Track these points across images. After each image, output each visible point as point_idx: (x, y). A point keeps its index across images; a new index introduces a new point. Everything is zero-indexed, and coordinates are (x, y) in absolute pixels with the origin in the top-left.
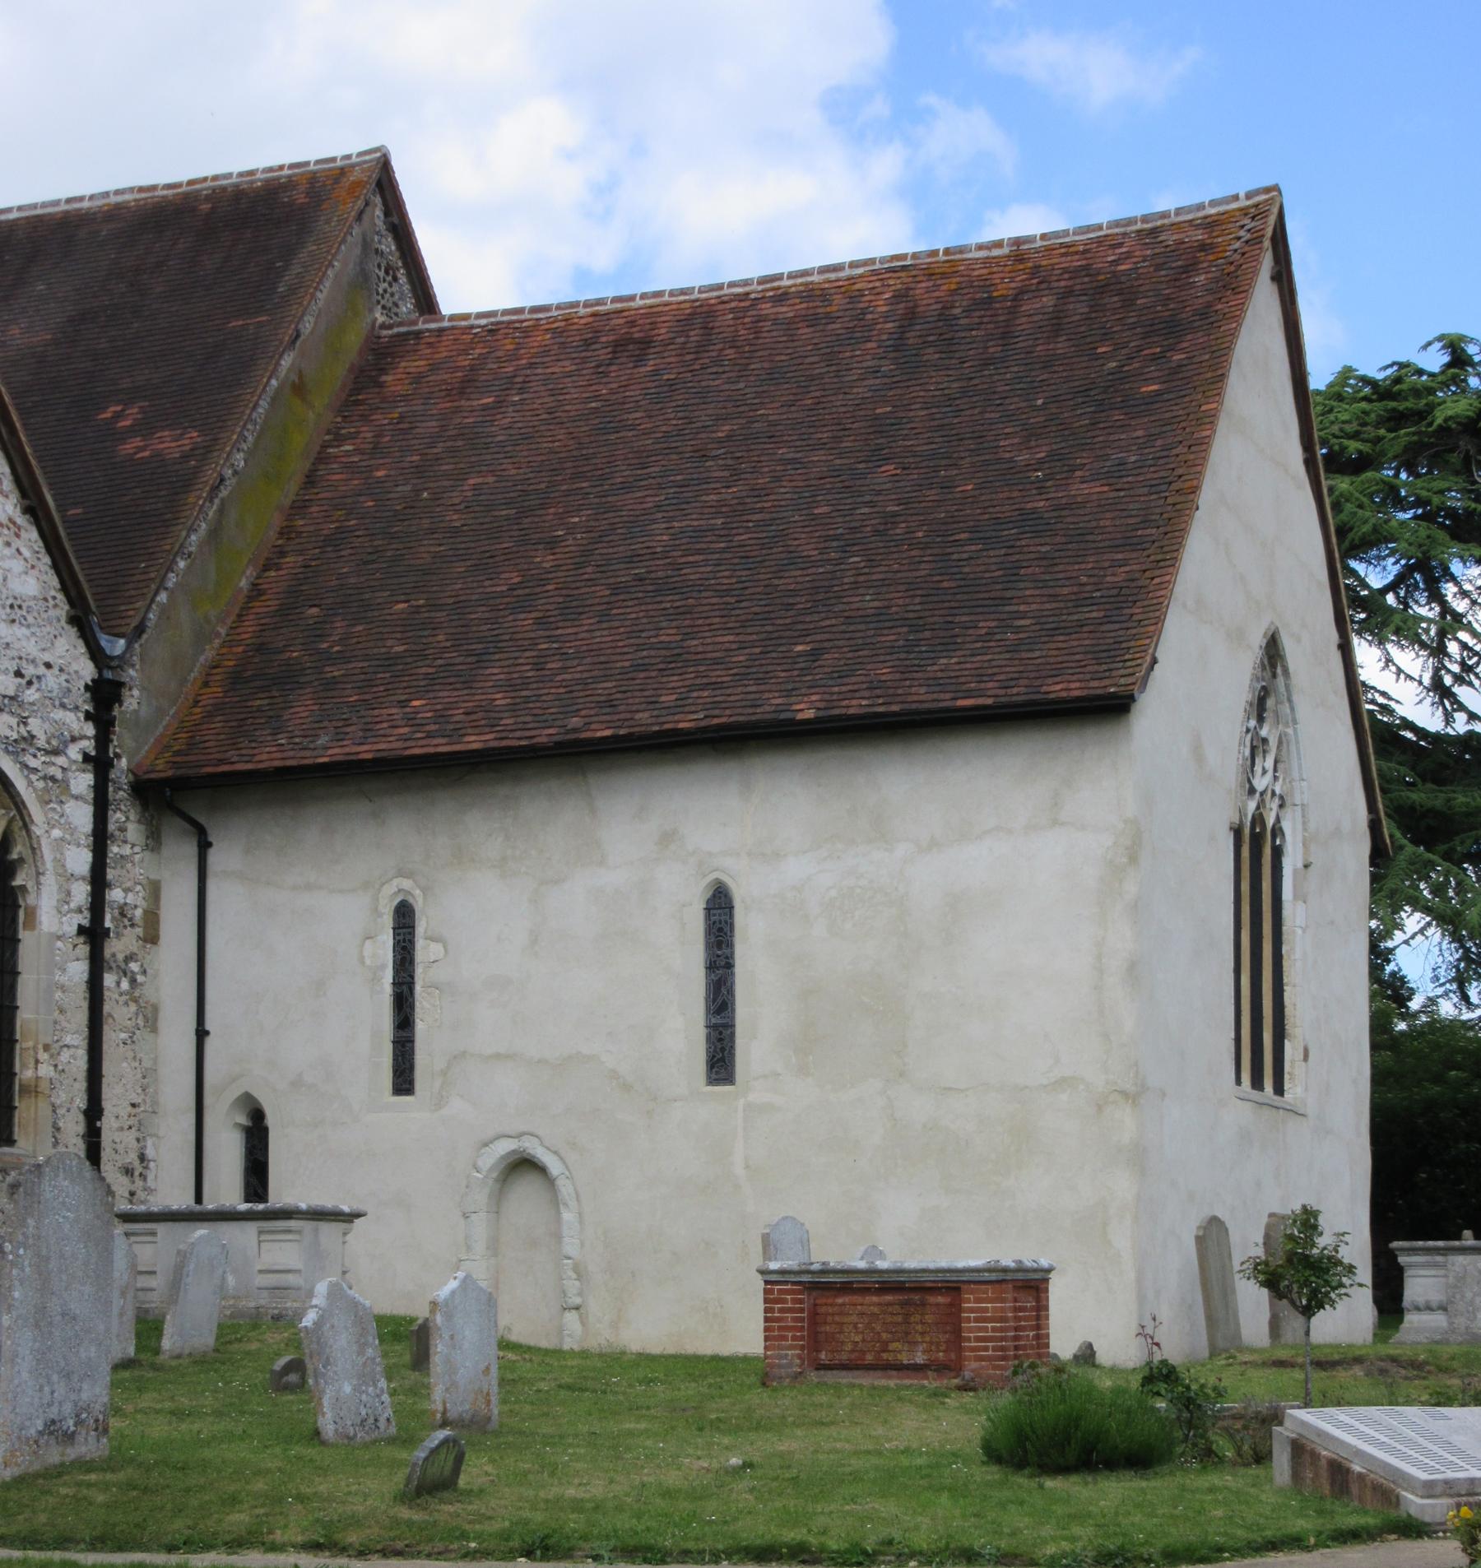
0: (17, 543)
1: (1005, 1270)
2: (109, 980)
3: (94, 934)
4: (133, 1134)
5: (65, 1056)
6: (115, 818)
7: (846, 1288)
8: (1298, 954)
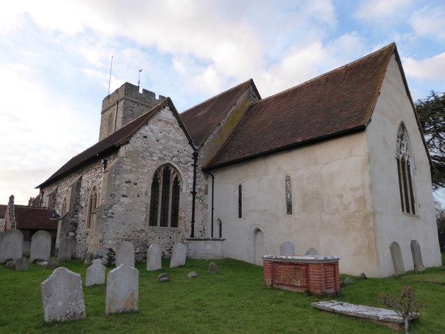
1: (320, 261)
2: (196, 200)
3: (194, 193)
6: (198, 175)
7: (281, 263)
8: (418, 195)
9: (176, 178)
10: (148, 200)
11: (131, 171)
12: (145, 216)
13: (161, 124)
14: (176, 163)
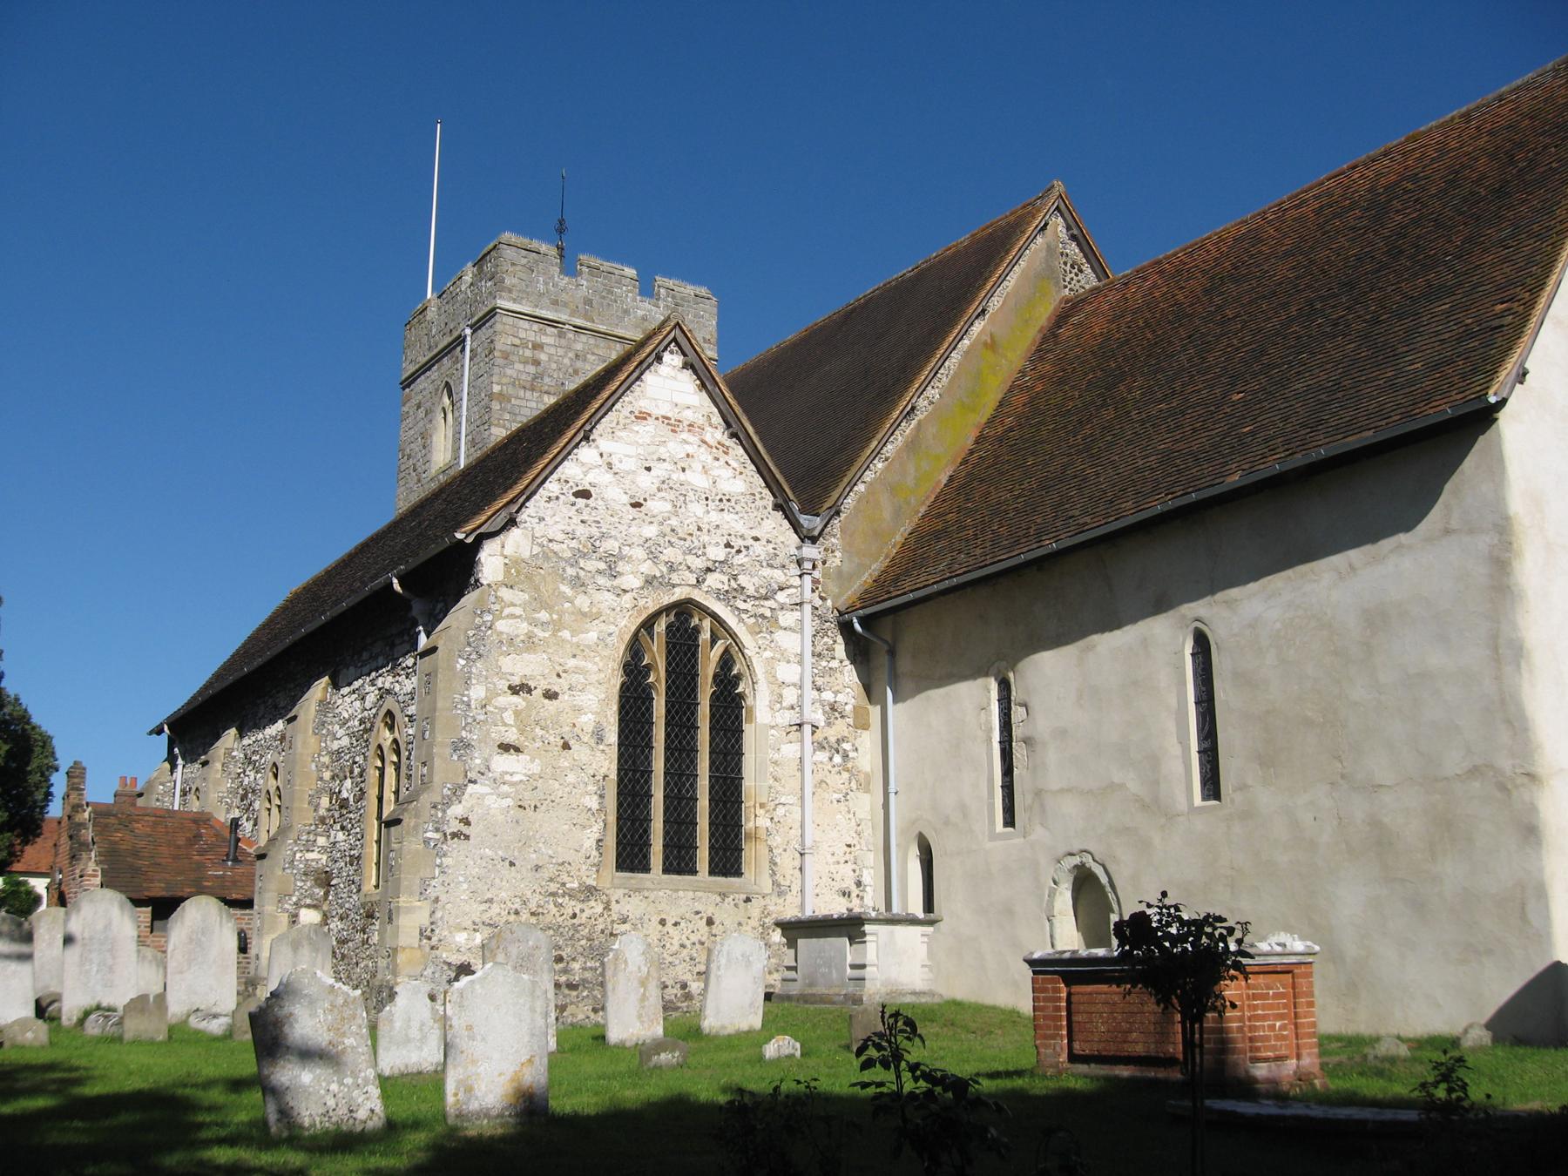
0: (726, 458)
4: (850, 866)
5: (781, 811)
9: (726, 661)
10: (606, 762)
11: (530, 643)
12: (594, 832)
13: (647, 430)
14: (725, 596)
